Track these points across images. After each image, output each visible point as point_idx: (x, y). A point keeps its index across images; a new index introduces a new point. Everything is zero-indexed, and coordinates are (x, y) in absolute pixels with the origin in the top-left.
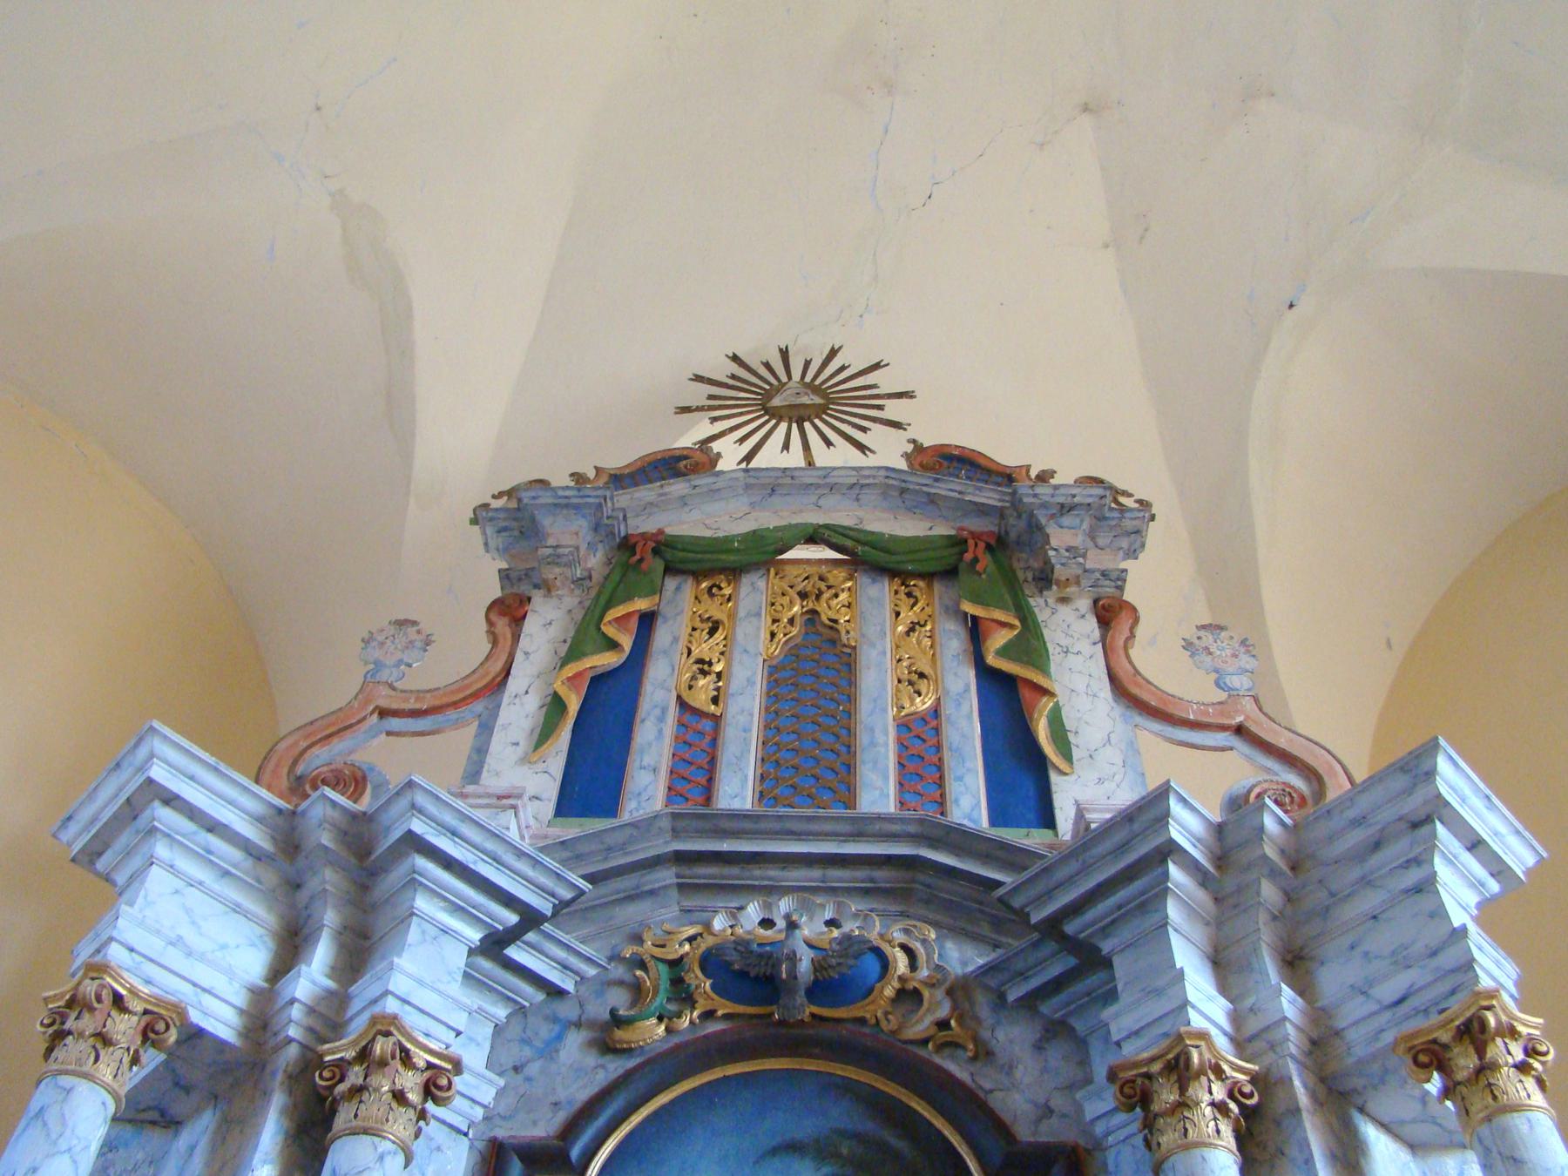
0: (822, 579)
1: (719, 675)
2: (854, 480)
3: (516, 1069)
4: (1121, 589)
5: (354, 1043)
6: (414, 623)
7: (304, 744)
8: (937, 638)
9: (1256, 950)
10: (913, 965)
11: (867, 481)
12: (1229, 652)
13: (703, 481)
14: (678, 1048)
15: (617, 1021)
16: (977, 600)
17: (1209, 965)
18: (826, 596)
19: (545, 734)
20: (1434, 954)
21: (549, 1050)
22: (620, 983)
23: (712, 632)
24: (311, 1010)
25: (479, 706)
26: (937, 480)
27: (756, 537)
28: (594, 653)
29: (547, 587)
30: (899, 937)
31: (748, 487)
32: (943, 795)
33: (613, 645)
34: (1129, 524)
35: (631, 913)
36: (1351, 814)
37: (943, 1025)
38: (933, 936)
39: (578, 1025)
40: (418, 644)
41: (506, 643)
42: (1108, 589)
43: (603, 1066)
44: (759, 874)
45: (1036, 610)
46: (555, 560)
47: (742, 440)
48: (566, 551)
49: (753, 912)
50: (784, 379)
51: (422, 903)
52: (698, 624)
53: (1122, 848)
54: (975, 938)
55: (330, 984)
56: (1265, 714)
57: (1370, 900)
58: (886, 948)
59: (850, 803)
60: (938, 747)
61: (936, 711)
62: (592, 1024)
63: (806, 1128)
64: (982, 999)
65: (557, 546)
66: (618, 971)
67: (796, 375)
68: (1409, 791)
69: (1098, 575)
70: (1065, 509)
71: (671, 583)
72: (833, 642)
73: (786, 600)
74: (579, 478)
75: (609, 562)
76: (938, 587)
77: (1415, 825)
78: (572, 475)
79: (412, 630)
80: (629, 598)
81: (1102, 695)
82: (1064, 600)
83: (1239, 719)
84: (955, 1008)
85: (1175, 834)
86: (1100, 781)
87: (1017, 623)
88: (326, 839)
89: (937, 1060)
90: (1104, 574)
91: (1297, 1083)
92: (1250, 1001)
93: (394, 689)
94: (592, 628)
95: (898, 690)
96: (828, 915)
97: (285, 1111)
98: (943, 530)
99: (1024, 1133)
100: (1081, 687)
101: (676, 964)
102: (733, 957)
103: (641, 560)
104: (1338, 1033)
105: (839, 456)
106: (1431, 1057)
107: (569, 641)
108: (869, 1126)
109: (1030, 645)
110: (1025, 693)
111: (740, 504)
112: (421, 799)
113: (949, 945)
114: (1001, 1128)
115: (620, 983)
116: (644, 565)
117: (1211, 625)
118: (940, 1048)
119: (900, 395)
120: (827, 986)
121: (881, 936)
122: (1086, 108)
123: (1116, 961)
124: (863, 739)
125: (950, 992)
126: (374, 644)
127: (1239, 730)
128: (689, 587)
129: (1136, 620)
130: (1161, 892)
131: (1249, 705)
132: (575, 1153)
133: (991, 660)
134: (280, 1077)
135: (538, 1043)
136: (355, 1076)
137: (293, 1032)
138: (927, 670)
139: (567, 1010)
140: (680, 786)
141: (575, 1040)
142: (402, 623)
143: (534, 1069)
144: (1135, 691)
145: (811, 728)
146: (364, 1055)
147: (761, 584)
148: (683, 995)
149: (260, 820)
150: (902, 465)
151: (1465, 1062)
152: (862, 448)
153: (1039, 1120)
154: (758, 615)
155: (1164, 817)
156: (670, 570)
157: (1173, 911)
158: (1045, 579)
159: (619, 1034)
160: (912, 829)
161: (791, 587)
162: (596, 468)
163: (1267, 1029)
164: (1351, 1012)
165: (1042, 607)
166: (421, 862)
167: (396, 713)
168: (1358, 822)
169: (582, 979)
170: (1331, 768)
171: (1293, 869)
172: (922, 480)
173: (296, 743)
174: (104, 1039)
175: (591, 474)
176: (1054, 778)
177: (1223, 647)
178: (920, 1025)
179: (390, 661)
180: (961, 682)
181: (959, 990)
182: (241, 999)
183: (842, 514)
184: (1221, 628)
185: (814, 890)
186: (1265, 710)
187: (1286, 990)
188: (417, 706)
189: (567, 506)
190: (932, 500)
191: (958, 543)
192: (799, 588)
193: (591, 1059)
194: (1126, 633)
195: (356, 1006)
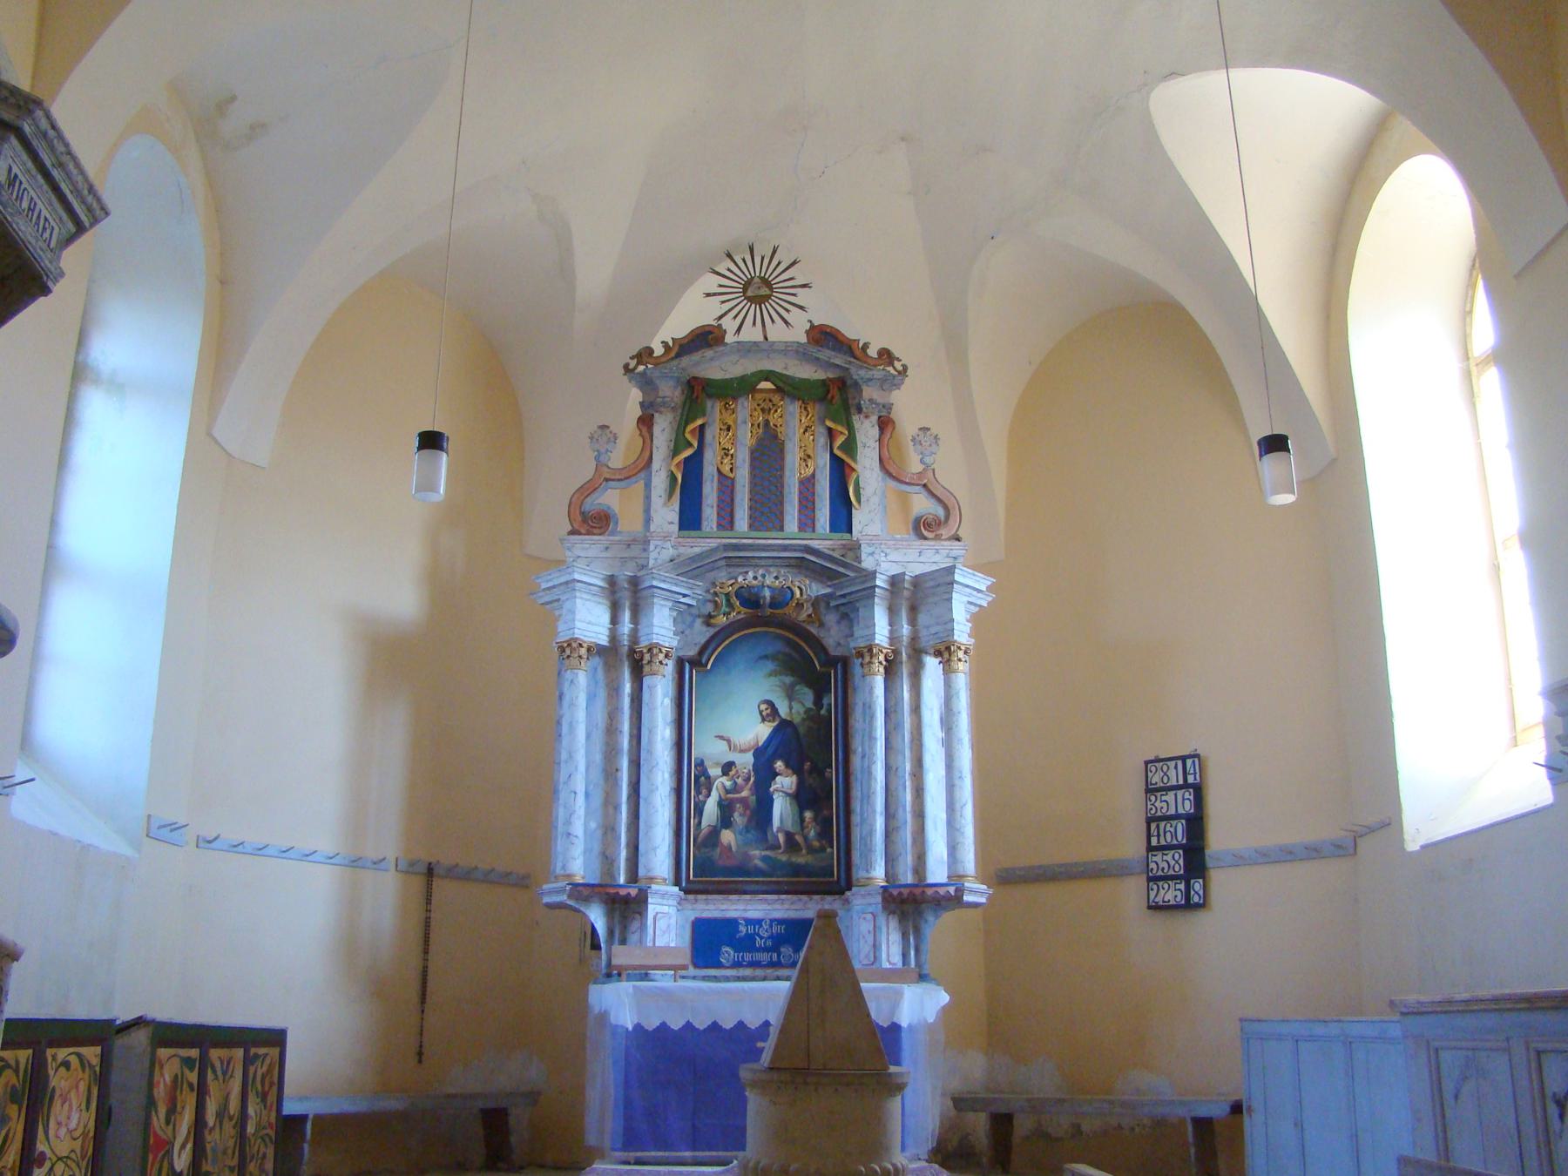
0: (770, 401)
1: (732, 455)
2: (783, 348)
3: (682, 633)
4: (890, 413)
5: (646, 647)
6: (608, 427)
7: (583, 497)
8: (816, 434)
9: (901, 608)
10: (801, 594)
11: (790, 349)
12: (928, 443)
13: (721, 348)
14: (732, 623)
15: (710, 616)
16: (834, 421)
17: (887, 611)
18: (772, 411)
19: (670, 495)
20: (945, 624)
21: (691, 626)
22: (710, 601)
23: (728, 429)
24: (629, 636)
25: (642, 475)
26: (819, 351)
27: (743, 378)
28: (684, 450)
29: (661, 413)
30: (797, 584)
31: (739, 351)
32: (814, 516)
33: (690, 445)
34: (896, 382)
35: (712, 575)
36: (931, 577)
37: (810, 616)
38: (808, 582)
39: (699, 616)
40: (612, 439)
41: (648, 441)
42: (884, 413)
43: (708, 631)
44: (753, 562)
45: (855, 422)
46: (664, 404)
47: (735, 317)
48: (668, 399)
49: (751, 574)
50: (753, 275)
51: (655, 600)
52: (722, 427)
53: (863, 582)
54: (822, 582)
55: (632, 626)
56: (935, 478)
57: (936, 599)
58: (793, 588)
59: (782, 529)
60: (814, 493)
61: (813, 475)
62: (704, 616)
63: (770, 650)
64: (823, 605)
65: (664, 397)
66: (709, 597)
67: (758, 274)
68: (948, 575)
69: (881, 406)
70: (870, 380)
71: (709, 403)
72: (776, 437)
73: (756, 414)
74: (665, 344)
75: (683, 391)
76: (817, 406)
77: (949, 584)
78: (662, 342)
79: (608, 431)
80: (695, 419)
81: (875, 469)
82: (867, 417)
83: (925, 481)
84: (813, 610)
85: (878, 583)
86: (870, 512)
87: (847, 432)
88: (626, 586)
89: (808, 627)
90: (884, 407)
91: (904, 654)
92: (895, 628)
93: (609, 468)
94: (682, 437)
95: (800, 465)
96: (775, 575)
97: (629, 667)
98: (820, 375)
99: (834, 652)
100: (868, 466)
101: (727, 595)
102: (746, 595)
103: (697, 397)
104: (919, 638)
105: (777, 333)
106: (938, 653)
107: (673, 441)
108: (787, 650)
109: (850, 446)
110: (847, 470)
111: (734, 358)
112: (655, 576)
113: (813, 584)
114: (824, 649)
115: (710, 601)
116: (699, 401)
117: (924, 428)
118: (809, 623)
119: (804, 286)
120: (773, 605)
121: (792, 582)
122: (903, 139)
123: (860, 610)
124: (786, 490)
125: (813, 605)
126: (594, 440)
127: (925, 486)
128: (718, 405)
129: (894, 429)
130: (873, 596)
131: (930, 474)
132: (704, 661)
133: (836, 451)
134: (625, 658)
135: (688, 623)
136: (647, 657)
137: (626, 643)
138: (812, 455)
139: (694, 611)
140: (723, 513)
141: (699, 621)
142: (604, 427)
143: (687, 632)
144: (888, 467)
145: (767, 483)
146: (650, 650)
147: (746, 404)
148: (730, 605)
149: (603, 579)
150: (803, 339)
151: (946, 655)
152: (786, 322)
153: (837, 647)
154: (745, 422)
155: (875, 578)
156: (710, 396)
157: (876, 600)
158: (860, 410)
159: (712, 621)
160: (803, 548)
161: (758, 405)
162: (672, 338)
163: (899, 637)
164: (923, 633)
165: (855, 418)
166: (655, 590)
167: (613, 480)
168: (932, 580)
169: (698, 600)
170: (954, 508)
171: (915, 587)
172: (814, 351)
173: (578, 498)
174: (580, 657)
175: (671, 344)
176: (853, 511)
177: (926, 440)
178: (803, 616)
179: (603, 450)
180: (824, 460)
181: (816, 603)
182: (607, 632)
183: (777, 365)
184: (928, 429)
185: (771, 566)
186: (936, 476)
187: (905, 626)
188: (620, 477)
189: (666, 377)
190: (817, 359)
191: (824, 383)
192: (761, 407)
193: (704, 628)
194: (889, 436)
195: (639, 635)
